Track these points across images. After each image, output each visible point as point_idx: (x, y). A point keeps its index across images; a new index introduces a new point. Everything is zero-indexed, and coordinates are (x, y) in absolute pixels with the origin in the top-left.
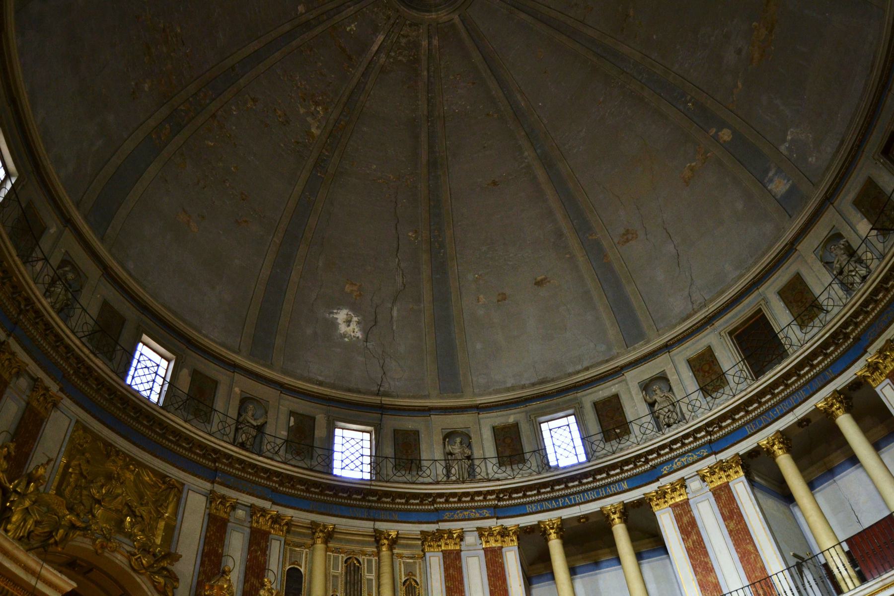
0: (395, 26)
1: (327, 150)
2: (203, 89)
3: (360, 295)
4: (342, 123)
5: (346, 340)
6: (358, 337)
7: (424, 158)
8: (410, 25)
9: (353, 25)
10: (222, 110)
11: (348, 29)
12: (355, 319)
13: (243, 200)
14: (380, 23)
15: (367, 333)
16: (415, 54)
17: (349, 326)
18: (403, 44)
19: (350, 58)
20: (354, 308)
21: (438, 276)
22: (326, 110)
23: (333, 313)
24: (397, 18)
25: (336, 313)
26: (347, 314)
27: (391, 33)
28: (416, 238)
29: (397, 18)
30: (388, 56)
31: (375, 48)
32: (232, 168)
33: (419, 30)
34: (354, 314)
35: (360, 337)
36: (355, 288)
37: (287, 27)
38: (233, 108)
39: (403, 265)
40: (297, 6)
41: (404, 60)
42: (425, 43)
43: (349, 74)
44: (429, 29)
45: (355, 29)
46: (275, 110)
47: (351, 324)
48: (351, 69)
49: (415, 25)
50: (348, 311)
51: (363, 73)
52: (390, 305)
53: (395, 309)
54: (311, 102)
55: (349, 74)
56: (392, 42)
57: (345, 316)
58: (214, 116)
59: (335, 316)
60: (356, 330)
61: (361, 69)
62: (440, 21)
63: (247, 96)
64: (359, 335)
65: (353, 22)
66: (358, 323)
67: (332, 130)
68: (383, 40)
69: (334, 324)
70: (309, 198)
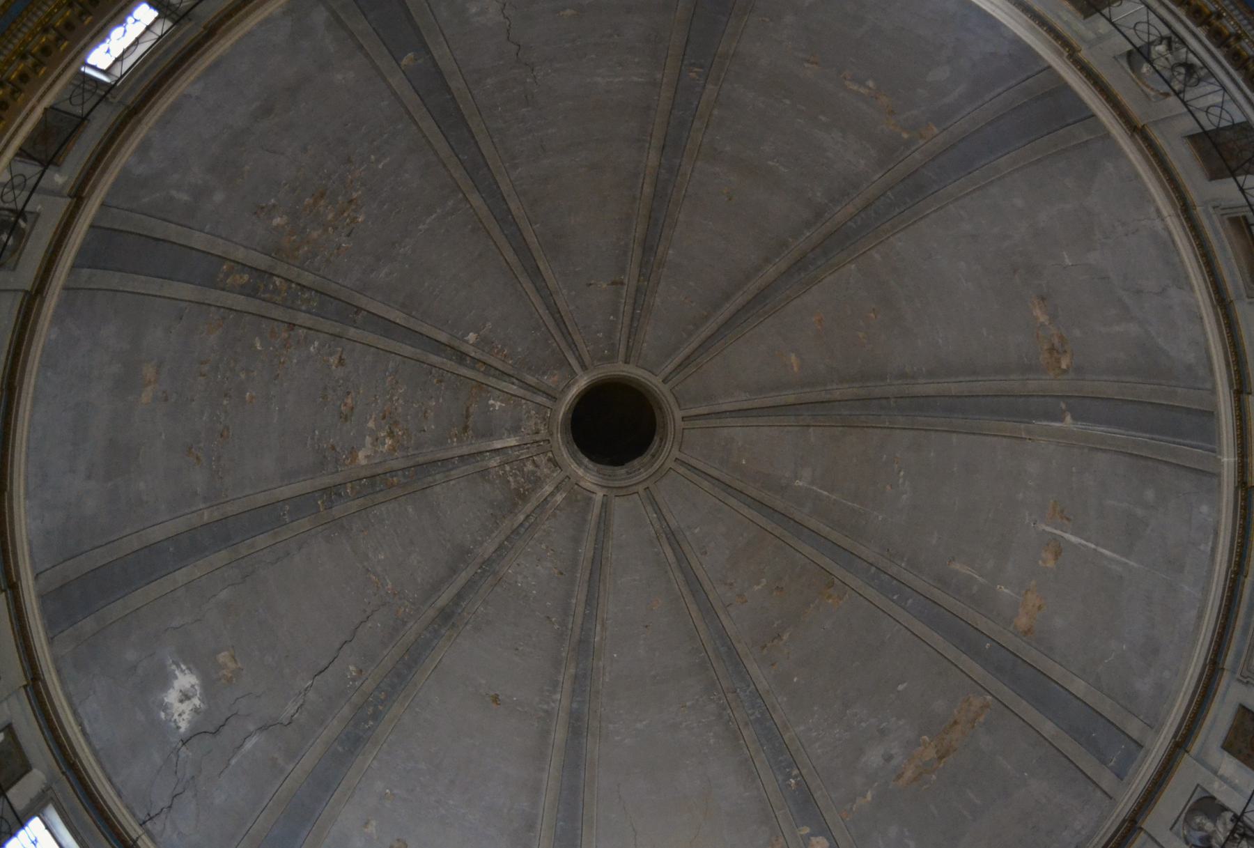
0: (535, 445)
1: (352, 488)
2: (313, 293)
3: (230, 680)
4: (395, 479)
5: (163, 715)
6: (178, 728)
7: (444, 599)
8: (550, 460)
9: (499, 403)
10: (305, 331)
11: (491, 402)
12: (196, 701)
13: (222, 436)
14: (525, 429)
15: (196, 733)
16: (528, 490)
17: (181, 701)
18: (525, 469)
19: (466, 428)
20: (210, 686)
21: (340, 749)
22: (393, 449)
23: (178, 666)
24: (544, 441)
25: (182, 671)
26: (193, 686)
27: (525, 447)
28: (354, 680)
29: (544, 441)
30: (501, 465)
31: (498, 445)
32: (248, 394)
33: (553, 472)
34: (201, 694)
35: (182, 730)
36: (232, 665)
37: (443, 337)
38: (316, 343)
39: (311, 695)
40: (471, 331)
41: (513, 484)
42: (548, 489)
43: (449, 441)
44: (563, 481)
45: (497, 408)
46: (349, 393)
47: (187, 702)
48: (455, 440)
49: (555, 463)
50: (197, 682)
51: (462, 456)
52: (252, 728)
53: (254, 740)
54: (387, 427)
55: (449, 441)
56: (519, 456)
57: (188, 686)
58: (292, 326)
59: (177, 672)
60: (185, 716)
61: (465, 450)
62: (582, 484)
63: (340, 349)
64: (184, 726)
65: (502, 401)
66: (196, 710)
67: (379, 475)
68: (511, 447)
69: (165, 681)
70: (284, 515)
